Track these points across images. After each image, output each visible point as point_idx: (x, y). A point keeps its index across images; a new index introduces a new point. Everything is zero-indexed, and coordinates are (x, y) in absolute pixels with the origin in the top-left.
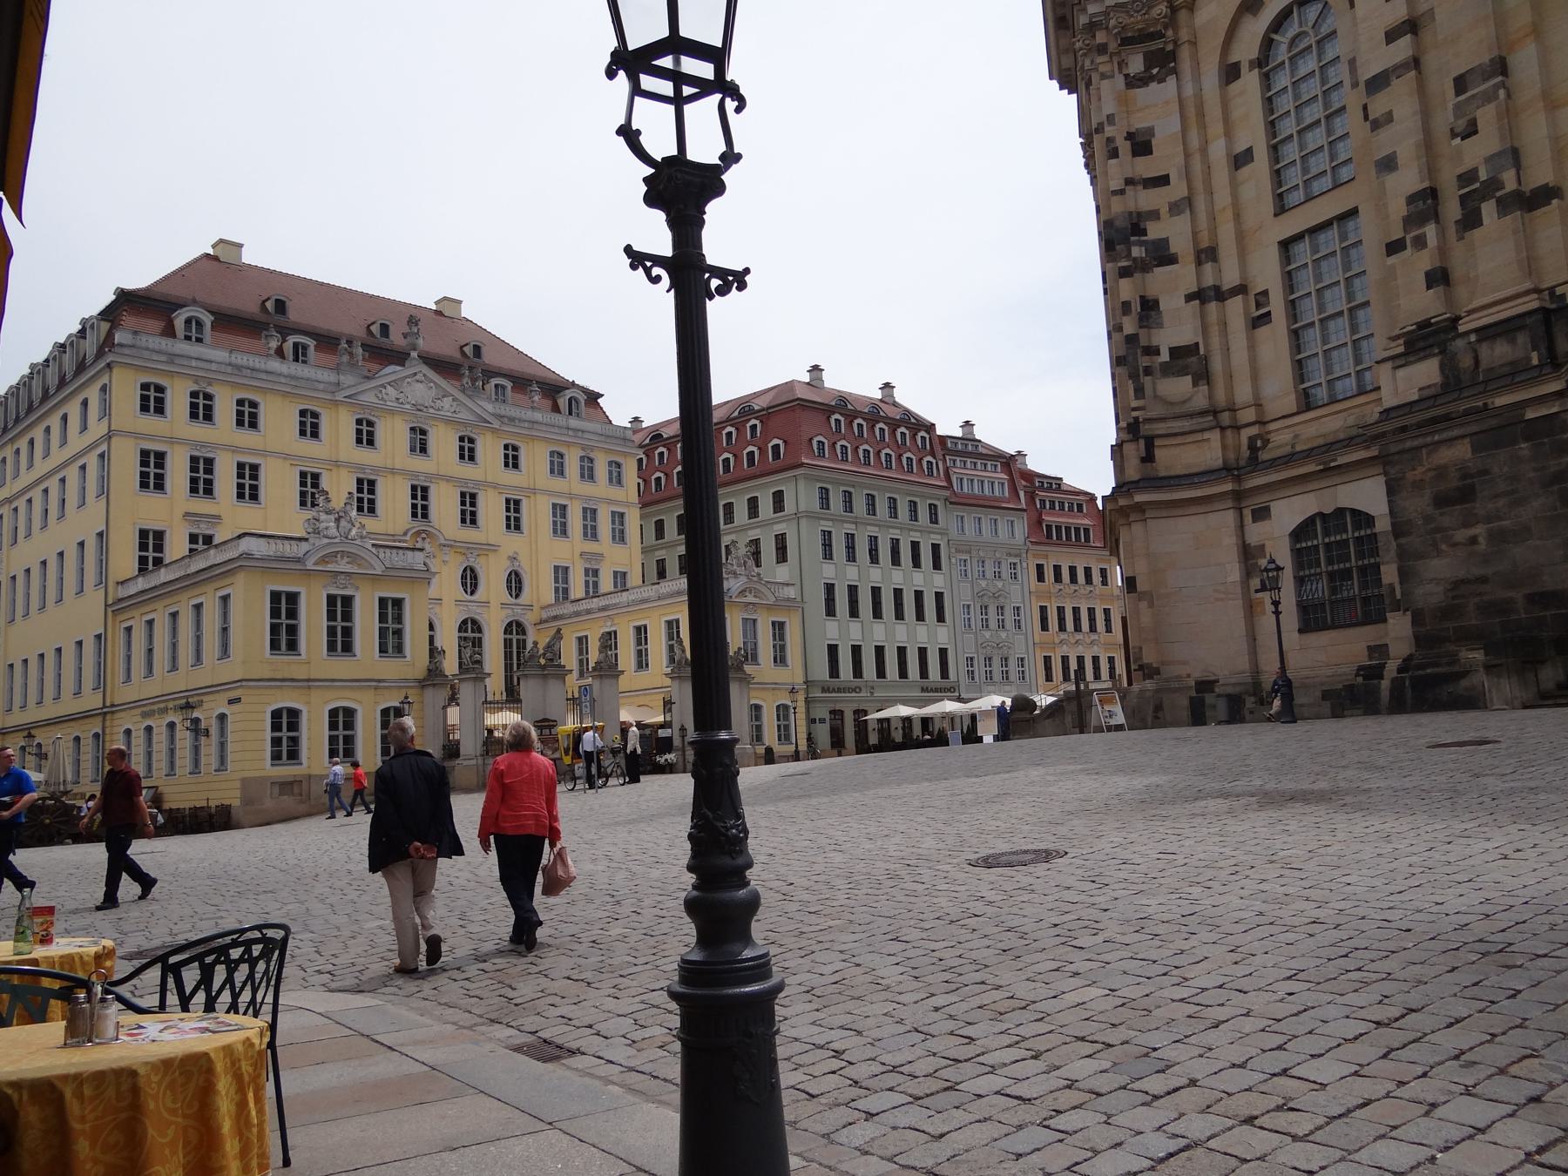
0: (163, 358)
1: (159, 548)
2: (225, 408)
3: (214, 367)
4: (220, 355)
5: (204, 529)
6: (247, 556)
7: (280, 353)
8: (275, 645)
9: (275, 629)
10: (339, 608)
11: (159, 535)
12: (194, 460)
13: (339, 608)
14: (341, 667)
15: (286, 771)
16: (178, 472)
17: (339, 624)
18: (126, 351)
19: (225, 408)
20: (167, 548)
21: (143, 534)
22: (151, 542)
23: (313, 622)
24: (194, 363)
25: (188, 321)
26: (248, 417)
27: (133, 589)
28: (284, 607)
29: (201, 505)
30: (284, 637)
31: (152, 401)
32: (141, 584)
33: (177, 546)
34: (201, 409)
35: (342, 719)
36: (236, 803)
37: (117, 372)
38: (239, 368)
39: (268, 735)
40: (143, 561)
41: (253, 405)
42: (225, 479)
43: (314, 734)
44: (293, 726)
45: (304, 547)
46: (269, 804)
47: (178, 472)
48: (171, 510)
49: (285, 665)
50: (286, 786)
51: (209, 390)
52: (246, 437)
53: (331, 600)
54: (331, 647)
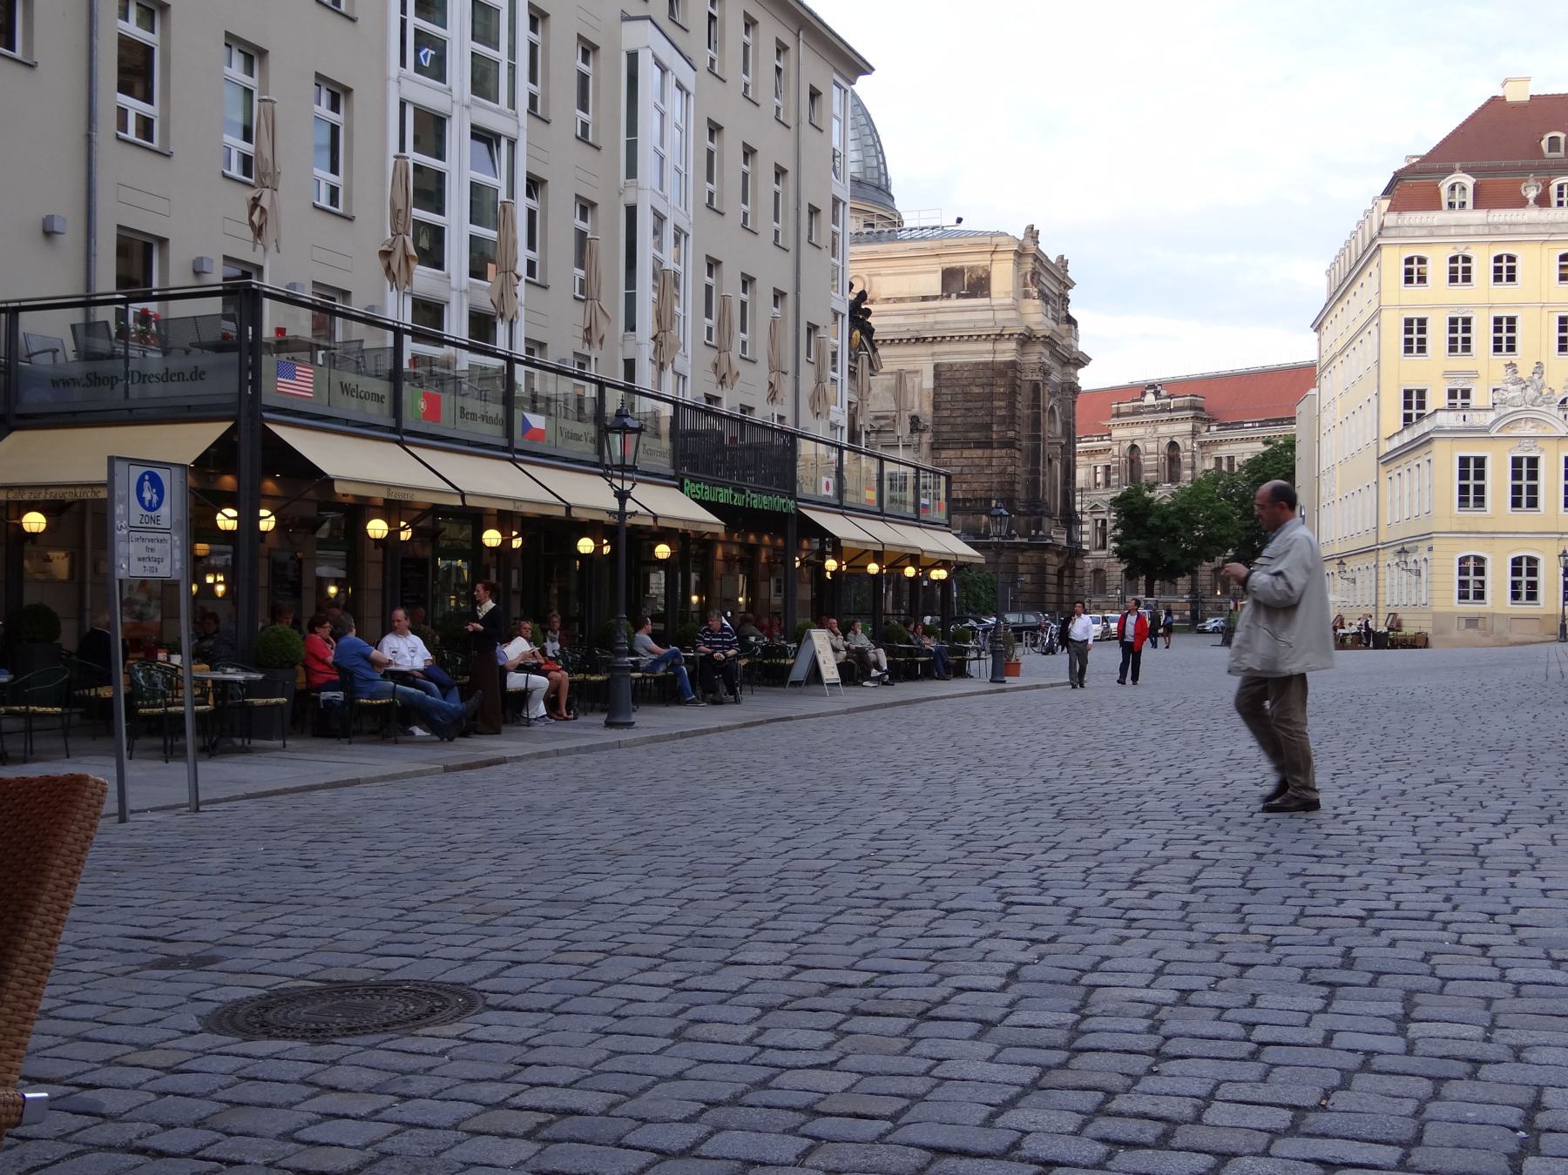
0: (1424, 232)
1: (1421, 405)
2: (1482, 268)
3: (1472, 230)
4: (1480, 216)
5: (1459, 385)
6: (1439, 430)
7: (1543, 201)
8: (1463, 501)
9: (1464, 489)
10: (1524, 469)
11: (1422, 394)
12: (1453, 321)
13: (1524, 469)
14: (1525, 519)
15: (1472, 608)
16: (1438, 335)
17: (1525, 482)
18: (1393, 232)
19: (1482, 268)
20: (1427, 405)
21: (1408, 394)
22: (1414, 400)
23: (1498, 481)
24: (1453, 231)
25: (1453, 188)
26: (1505, 271)
27: (1396, 442)
28: (1473, 469)
29: (1460, 362)
30: (1471, 491)
31: (1414, 274)
32: (1407, 437)
33: (1437, 399)
34: (1460, 272)
35: (1525, 568)
36: (1430, 631)
37: (1385, 250)
38: (1497, 225)
39: (1456, 578)
40: (1407, 418)
41: (1511, 259)
42: (1482, 334)
43: (1498, 579)
44: (1480, 571)
45: (1492, 416)
46: (1456, 634)
47: (1438, 335)
48: (1433, 370)
49: (1471, 516)
50: (1472, 622)
51: (1467, 253)
52: (1505, 290)
53: (1517, 462)
54: (1516, 503)
